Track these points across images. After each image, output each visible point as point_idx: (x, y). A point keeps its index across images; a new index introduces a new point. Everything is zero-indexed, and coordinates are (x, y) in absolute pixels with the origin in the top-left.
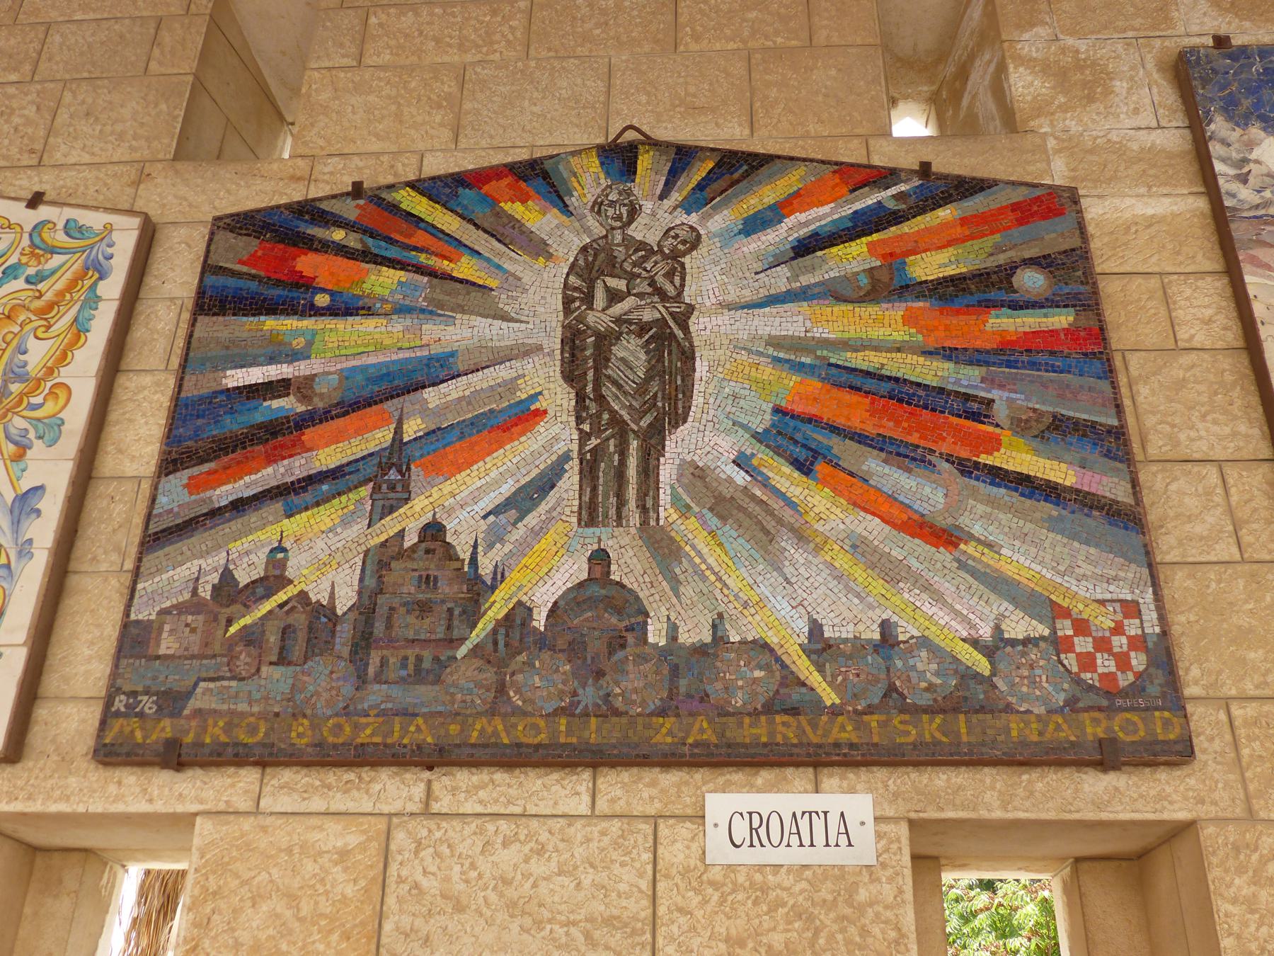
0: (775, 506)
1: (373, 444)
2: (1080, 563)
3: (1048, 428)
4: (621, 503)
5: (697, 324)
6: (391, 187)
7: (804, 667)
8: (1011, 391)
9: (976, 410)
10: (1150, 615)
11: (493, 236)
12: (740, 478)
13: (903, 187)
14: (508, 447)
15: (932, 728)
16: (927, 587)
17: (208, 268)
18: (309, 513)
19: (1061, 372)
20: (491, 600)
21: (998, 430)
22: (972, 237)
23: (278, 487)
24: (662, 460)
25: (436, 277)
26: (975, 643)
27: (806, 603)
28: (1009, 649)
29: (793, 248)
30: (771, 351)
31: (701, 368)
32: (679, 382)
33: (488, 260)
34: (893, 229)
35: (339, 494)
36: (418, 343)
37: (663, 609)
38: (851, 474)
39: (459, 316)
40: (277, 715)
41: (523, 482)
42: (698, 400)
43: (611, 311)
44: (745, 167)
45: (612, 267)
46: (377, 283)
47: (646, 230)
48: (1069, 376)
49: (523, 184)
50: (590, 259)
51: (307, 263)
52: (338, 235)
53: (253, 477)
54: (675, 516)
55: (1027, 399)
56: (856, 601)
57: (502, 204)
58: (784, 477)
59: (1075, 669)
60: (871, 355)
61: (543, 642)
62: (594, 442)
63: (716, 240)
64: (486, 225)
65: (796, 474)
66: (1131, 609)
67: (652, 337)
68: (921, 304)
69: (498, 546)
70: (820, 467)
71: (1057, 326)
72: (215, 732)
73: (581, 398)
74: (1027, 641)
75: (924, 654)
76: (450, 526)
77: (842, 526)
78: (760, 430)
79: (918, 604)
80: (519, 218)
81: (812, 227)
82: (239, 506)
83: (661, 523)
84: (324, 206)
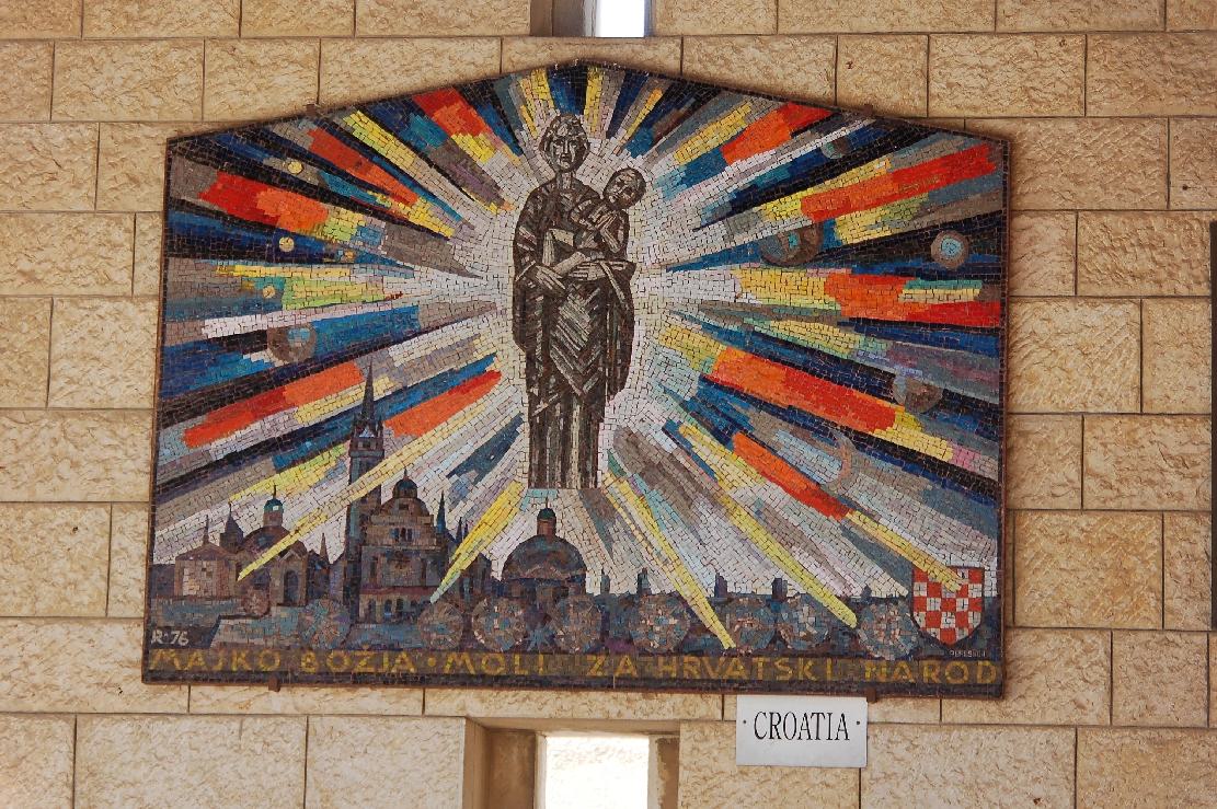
0: (696, 473)
1: (347, 401)
2: (943, 533)
3: (937, 406)
4: (566, 467)
5: (636, 284)
6: (344, 109)
7: (709, 617)
8: (912, 366)
9: (879, 384)
10: (991, 580)
11: (446, 175)
12: (668, 445)
13: (843, 132)
14: (466, 409)
15: (805, 669)
16: (814, 552)
17: (171, 203)
18: (297, 468)
19: (958, 348)
20: (457, 552)
21: (893, 406)
22: (901, 196)
23: (266, 442)
24: (601, 425)
25: (394, 222)
26: (847, 601)
27: (714, 562)
28: (873, 606)
29: (731, 202)
30: (702, 316)
31: (639, 330)
32: (618, 347)
33: (443, 205)
34: (827, 182)
35: (322, 451)
36: (381, 297)
37: (598, 564)
38: (763, 445)
39: (417, 268)
40: (289, 648)
41: (480, 444)
42: (634, 366)
43: (557, 268)
44: (693, 100)
45: (559, 216)
46: (337, 227)
47: (593, 175)
48: (966, 353)
49: (473, 112)
50: (540, 207)
51: (270, 201)
52: (295, 167)
53: (244, 432)
54: (611, 480)
55: (925, 376)
56: (756, 561)
57: (454, 137)
58: (705, 445)
59: (922, 625)
60: (792, 324)
61: (500, 590)
62: (542, 406)
63: (660, 189)
64: (440, 163)
65: (716, 443)
66: (977, 575)
67: (595, 297)
68: (843, 271)
69: (461, 503)
70: (737, 437)
71: (964, 299)
72: (239, 662)
73: (530, 360)
74: (889, 600)
75: (806, 608)
76: (420, 482)
77: (751, 494)
78: (688, 399)
79: (806, 565)
80: (471, 154)
81: (752, 177)
82: (235, 460)
83: (599, 485)
84: (277, 130)
